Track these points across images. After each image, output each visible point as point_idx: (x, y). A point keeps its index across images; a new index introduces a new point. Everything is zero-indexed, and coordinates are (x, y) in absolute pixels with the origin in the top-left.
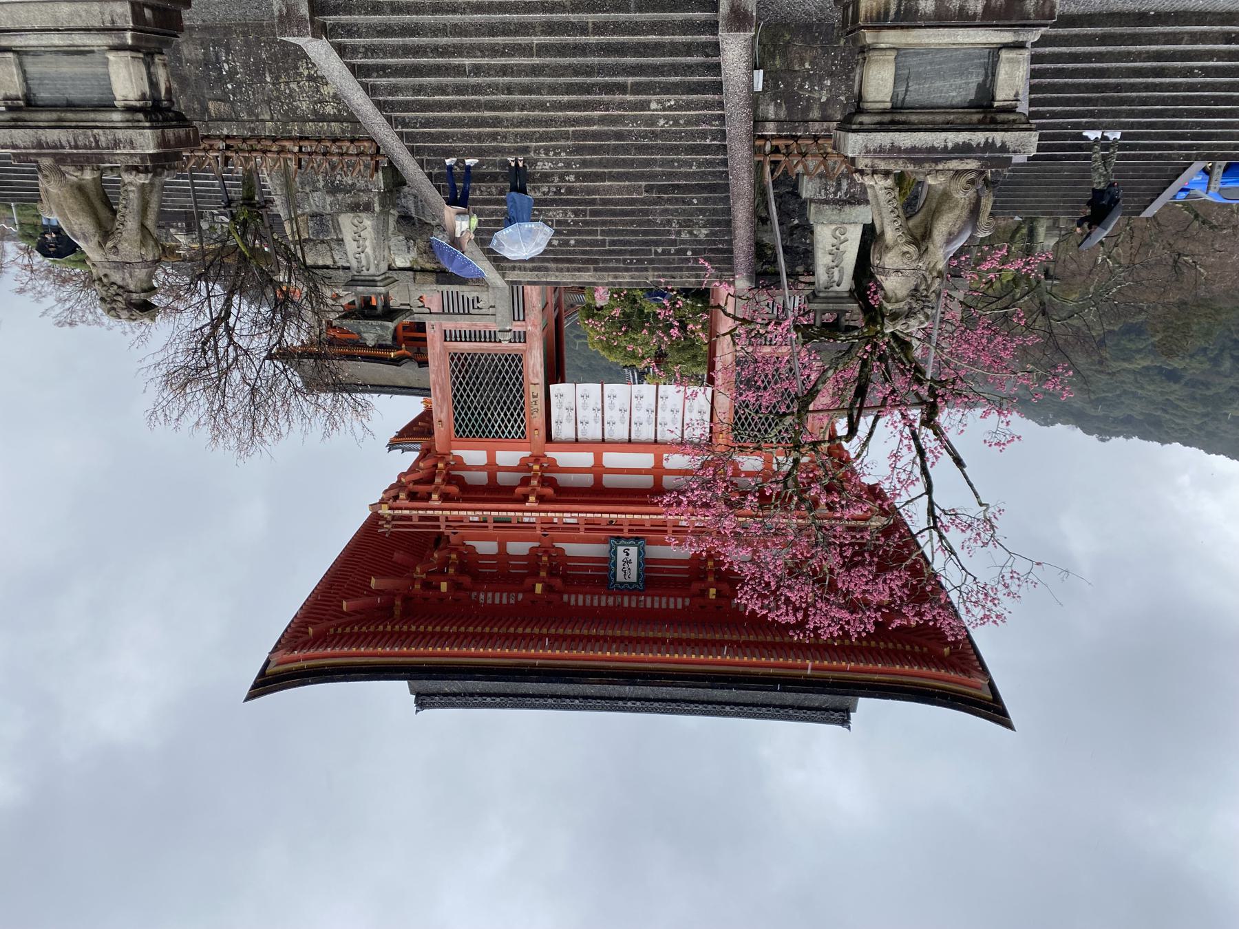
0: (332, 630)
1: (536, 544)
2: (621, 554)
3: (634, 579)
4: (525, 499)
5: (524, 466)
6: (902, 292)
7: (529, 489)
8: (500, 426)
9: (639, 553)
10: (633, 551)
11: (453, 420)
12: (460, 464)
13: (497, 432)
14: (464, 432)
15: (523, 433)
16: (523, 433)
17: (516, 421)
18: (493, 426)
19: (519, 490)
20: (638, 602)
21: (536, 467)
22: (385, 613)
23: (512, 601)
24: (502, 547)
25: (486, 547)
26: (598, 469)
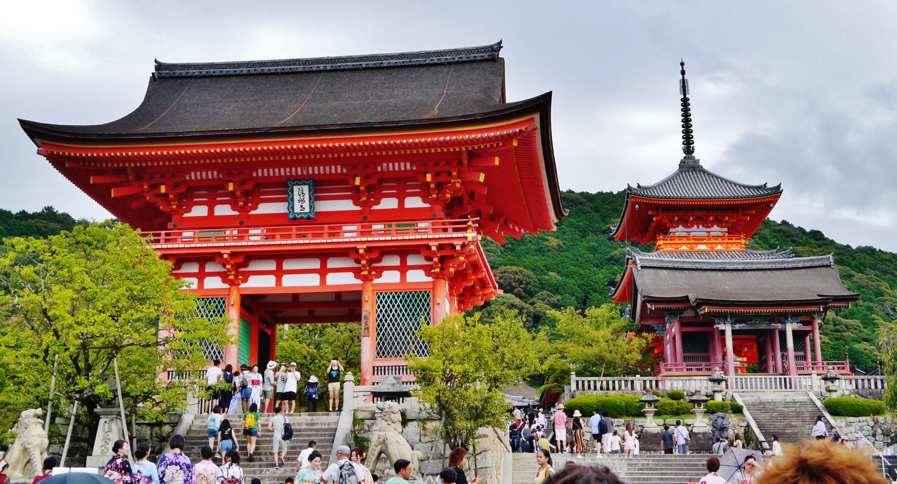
0: (501, 144)
1: (375, 208)
2: (306, 205)
3: (296, 188)
4: (368, 250)
5: (379, 272)
6: (32, 426)
7: (367, 257)
8: (396, 301)
9: (293, 208)
10: (297, 209)
11: (431, 304)
12: (427, 270)
13: (398, 297)
14: (423, 296)
15: (379, 297)
16: (379, 297)
17: (384, 306)
18: (401, 301)
19: (375, 255)
20: (291, 171)
21: (365, 273)
22: (471, 154)
23: (385, 165)
24: (401, 203)
25: (414, 203)
26: (323, 272)
